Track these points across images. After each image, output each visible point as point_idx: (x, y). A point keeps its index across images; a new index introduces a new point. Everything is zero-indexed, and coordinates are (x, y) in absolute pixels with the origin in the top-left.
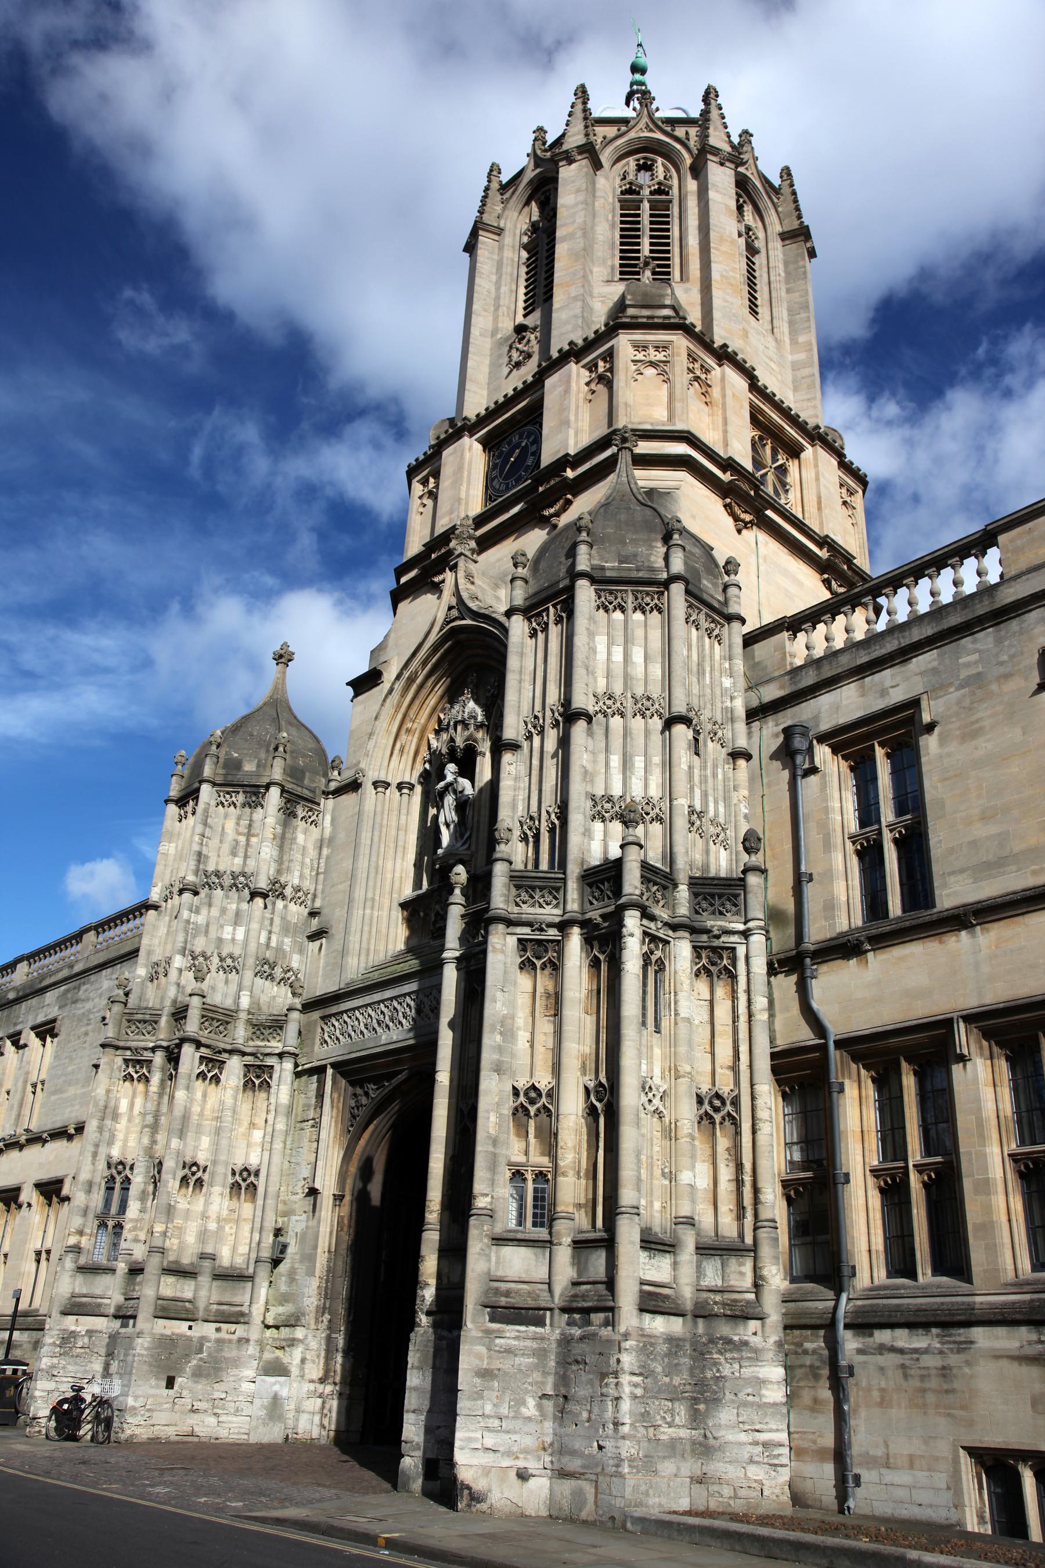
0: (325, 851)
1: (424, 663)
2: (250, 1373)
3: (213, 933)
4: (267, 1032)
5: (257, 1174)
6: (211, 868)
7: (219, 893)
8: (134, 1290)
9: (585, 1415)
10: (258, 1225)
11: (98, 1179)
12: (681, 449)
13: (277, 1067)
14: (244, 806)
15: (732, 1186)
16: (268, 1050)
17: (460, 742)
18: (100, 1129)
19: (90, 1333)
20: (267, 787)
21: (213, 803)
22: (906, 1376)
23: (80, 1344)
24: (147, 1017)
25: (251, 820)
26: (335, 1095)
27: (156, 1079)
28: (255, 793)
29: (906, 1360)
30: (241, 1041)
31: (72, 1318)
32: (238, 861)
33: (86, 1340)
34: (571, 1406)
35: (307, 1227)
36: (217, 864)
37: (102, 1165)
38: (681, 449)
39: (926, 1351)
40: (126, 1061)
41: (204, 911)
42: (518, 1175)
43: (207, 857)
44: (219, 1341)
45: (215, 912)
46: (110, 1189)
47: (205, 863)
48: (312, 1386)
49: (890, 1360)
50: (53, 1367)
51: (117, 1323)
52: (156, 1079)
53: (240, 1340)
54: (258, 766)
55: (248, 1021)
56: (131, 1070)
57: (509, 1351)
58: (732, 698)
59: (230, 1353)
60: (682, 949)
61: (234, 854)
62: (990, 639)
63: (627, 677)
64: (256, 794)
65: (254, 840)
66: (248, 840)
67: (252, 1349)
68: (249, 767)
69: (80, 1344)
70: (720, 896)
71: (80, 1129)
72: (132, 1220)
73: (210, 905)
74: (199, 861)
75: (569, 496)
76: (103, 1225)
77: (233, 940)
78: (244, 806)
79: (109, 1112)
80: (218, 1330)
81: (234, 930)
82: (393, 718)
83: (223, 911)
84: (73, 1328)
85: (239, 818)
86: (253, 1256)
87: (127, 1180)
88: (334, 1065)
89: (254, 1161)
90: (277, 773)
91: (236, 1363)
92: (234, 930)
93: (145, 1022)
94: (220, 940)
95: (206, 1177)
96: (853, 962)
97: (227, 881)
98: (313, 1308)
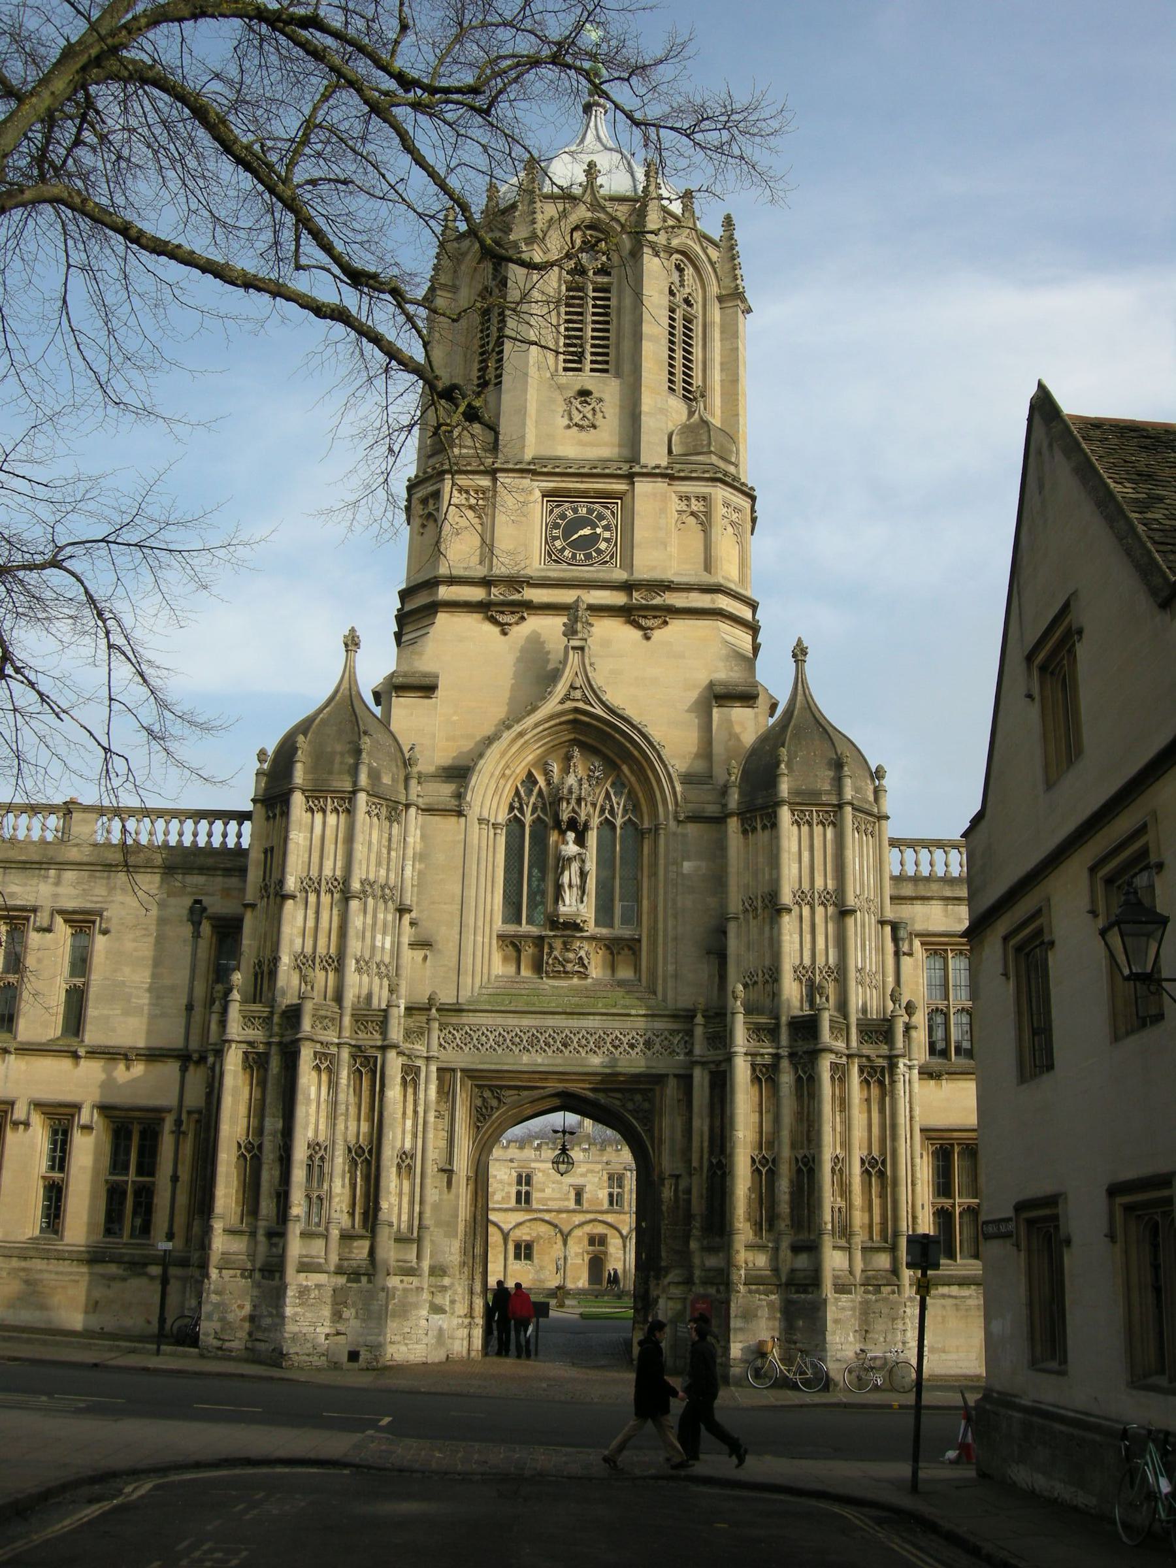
0: (417, 866)
1: (536, 725)
2: (424, 1312)
8: (351, 1252)
9: (882, 1339)
10: (417, 1199)
13: (423, 1069)
16: (418, 1054)
17: (583, 818)
19: (318, 1286)
20: (407, 806)
22: (957, 1310)
23: (312, 1296)
24: (329, 1014)
26: (464, 1095)
29: (957, 1302)
31: (303, 1275)
33: (317, 1292)
34: (869, 1336)
35: (440, 1200)
39: (970, 1297)
44: (405, 1290)
48: (460, 1321)
49: (950, 1301)
50: (296, 1314)
51: (341, 1280)
53: (417, 1288)
57: (843, 1309)
59: (412, 1299)
67: (425, 1295)
69: (312, 1296)
72: (339, 1195)
77: (383, 948)
80: (402, 1281)
82: (498, 763)
84: (305, 1283)
86: (416, 1223)
88: (462, 1070)
89: (408, 1146)
91: (416, 1306)
96: (932, 1082)
98: (457, 1263)
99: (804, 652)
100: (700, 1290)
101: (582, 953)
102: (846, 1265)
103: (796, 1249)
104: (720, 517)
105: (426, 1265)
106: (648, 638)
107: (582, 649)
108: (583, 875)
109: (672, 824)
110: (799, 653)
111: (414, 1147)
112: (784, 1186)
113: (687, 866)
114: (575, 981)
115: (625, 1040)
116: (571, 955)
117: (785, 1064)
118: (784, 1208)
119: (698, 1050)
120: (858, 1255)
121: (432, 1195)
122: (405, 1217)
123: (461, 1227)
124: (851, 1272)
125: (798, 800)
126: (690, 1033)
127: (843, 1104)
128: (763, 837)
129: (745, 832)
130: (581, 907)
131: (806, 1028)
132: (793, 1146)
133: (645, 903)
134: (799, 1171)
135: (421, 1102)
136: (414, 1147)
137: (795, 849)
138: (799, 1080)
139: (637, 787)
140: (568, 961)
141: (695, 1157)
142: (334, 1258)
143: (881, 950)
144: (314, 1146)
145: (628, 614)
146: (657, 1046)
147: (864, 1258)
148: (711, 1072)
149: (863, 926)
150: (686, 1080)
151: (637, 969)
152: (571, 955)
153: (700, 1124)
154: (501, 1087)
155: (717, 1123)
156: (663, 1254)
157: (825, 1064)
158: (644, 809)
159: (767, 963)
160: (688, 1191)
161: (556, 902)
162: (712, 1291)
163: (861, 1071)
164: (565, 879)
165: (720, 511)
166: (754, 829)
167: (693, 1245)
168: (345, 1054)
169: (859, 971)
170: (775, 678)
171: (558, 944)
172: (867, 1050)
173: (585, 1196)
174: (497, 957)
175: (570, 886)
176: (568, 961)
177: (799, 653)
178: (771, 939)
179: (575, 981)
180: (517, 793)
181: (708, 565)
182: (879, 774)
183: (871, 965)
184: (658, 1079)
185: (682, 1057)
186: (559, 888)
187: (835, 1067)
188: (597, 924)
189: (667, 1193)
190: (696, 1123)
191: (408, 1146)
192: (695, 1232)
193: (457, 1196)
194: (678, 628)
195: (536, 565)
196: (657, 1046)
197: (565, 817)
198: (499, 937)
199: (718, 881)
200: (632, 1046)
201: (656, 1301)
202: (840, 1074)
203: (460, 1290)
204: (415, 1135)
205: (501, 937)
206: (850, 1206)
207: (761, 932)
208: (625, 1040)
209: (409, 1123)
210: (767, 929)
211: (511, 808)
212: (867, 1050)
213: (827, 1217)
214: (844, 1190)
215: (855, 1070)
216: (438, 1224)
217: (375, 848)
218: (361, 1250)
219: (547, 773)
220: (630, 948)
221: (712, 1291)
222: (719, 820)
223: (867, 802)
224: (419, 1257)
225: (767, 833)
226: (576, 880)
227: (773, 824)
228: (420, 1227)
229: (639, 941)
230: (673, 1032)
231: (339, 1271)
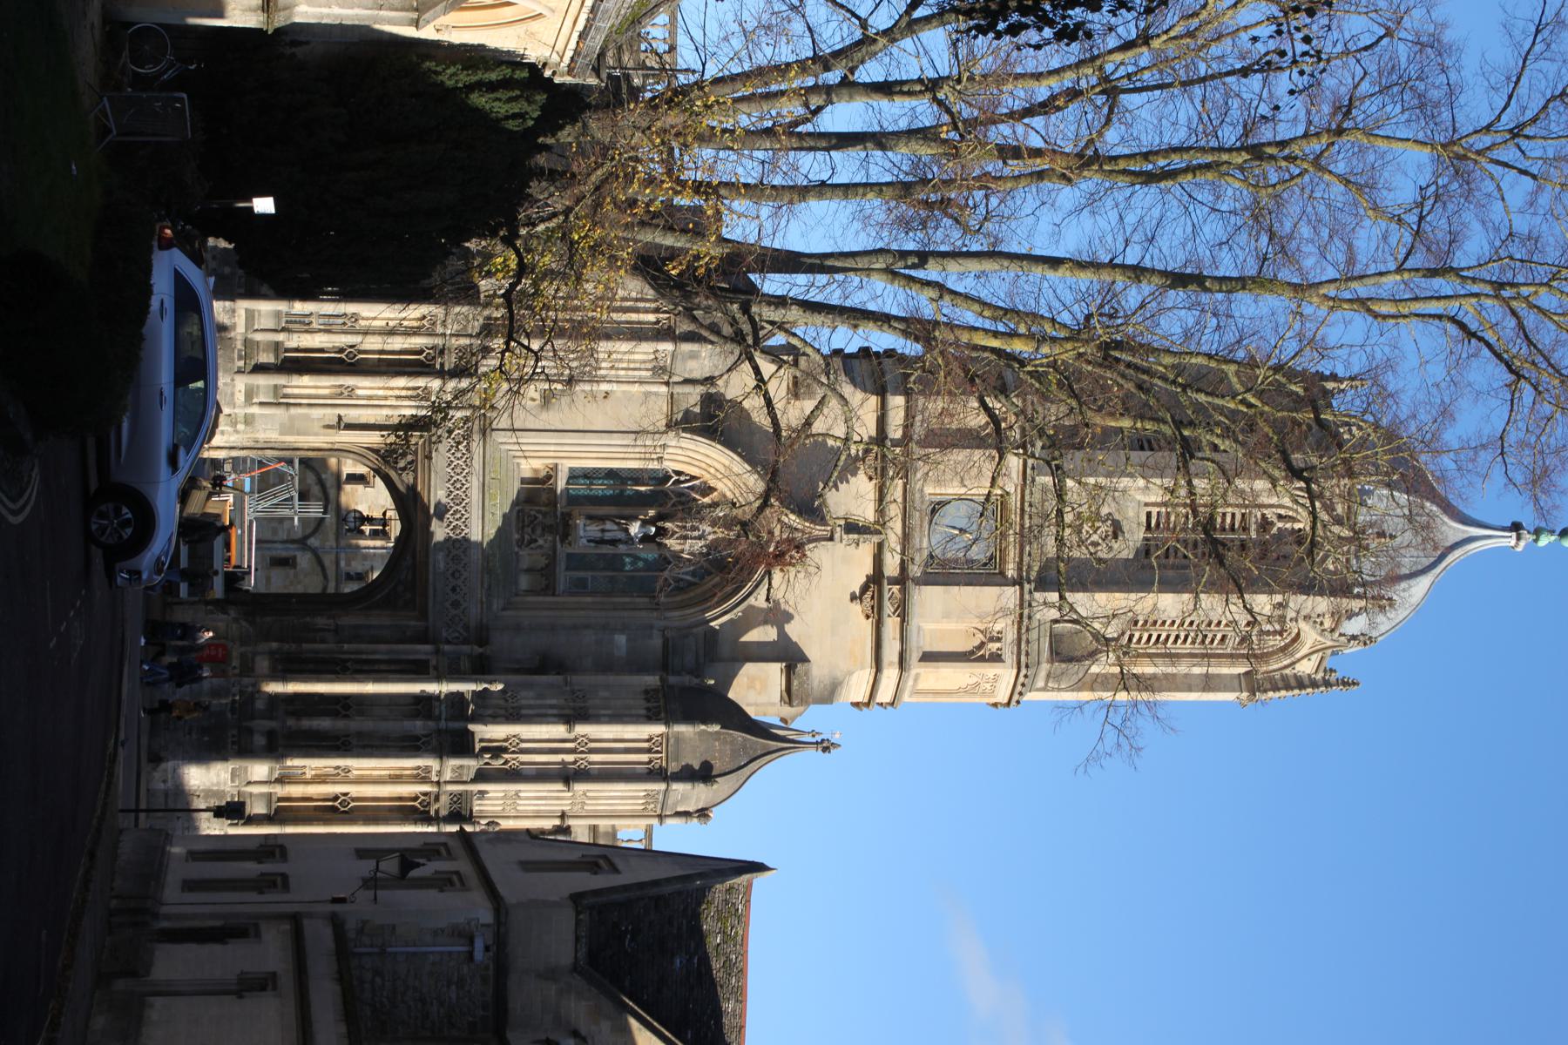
99: (825, 749)
100: (235, 654)
101: (541, 542)
102: (255, 778)
103: (270, 735)
104: (982, 671)
105: (255, 410)
106: (853, 598)
107: (831, 539)
108: (614, 542)
109: (662, 623)
110: (826, 746)
111: (359, 398)
112: (324, 724)
113: (621, 640)
114: (516, 536)
115: (459, 582)
116: (539, 531)
117: (431, 724)
118: (306, 723)
119: (447, 648)
120: (264, 789)
121: (316, 413)
122: (296, 391)
123: (290, 439)
124: (249, 783)
125: (672, 741)
126: (466, 642)
127: (396, 779)
128: (640, 705)
129: (646, 692)
130: (584, 541)
131: (461, 745)
132: (360, 734)
133: (589, 599)
134: (337, 738)
135: (399, 403)
136: (359, 398)
137: (626, 736)
138: (417, 738)
139: (699, 591)
140: (533, 531)
141: (354, 646)
142: (259, 337)
143: (538, 816)
144: (355, 317)
145: (876, 579)
146: (454, 612)
147: (262, 795)
148: (427, 662)
149: (558, 798)
150: (423, 637)
151: (531, 592)
152: (539, 531)
153: (382, 651)
154: (415, 471)
155: (383, 667)
156: (268, 619)
157: (432, 763)
158: (678, 598)
159: (524, 712)
160: (323, 641)
161: (590, 517)
162: (236, 663)
163: (425, 794)
164: (609, 525)
165: (990, 670)
166: (648, 700)
167: (275, 645)
168: (439, 341)
169: (517, 793)
170: (809, 719)
171: (549, 521)
172: (444, 799)
173: (360, 488)
174: (538, 464)
175: (603, 531)
176: (533, 531)
177: (826, 746)
178: (546, 715)
179: (516, 536)
180: (693, 478)
181: (929, 657)
182: (703, 813)
183: (525, 806)
184: (424, 615)
185: (444, 634)
186: (602, 519)
187: (428, 769)
188: (570, 556)
189: (321, 621)
190: (383, 647)
191: (359, 392)
192: (286, 646)
193: (316, 434)
194: (867, 626)
195: (929, 490)
196: (454, 612)
197: (668, 525)
198: (555, 468)
199: (607, 665)
200: (454, 590)
201: (226, 613)
202: (421, 777)
203: (232, 438)
204: (370, 398)
205: (555, 468)
206: (307, 783)
207: (552, 707)
208: (459, 582)
209: (381, 393)
210: (555, 712)
211: (679, 473)
212: (444, 799)
213: (297, 762)
214: (320, 779)
215: (426, 788)
216: (292, 418)
217: (626, 357)
218: (266, 358)
219: (715, 505)
220: (547, 587)
221: (236, 663)
222: (665, 666)
223: (676, 804)
224: (261, 404)
225: (643, 712)
226: (608, 536)
227: (651, 718)
228: (288, 405)
229: (554, 595)
230: (466, 627)
231: (246, 341)
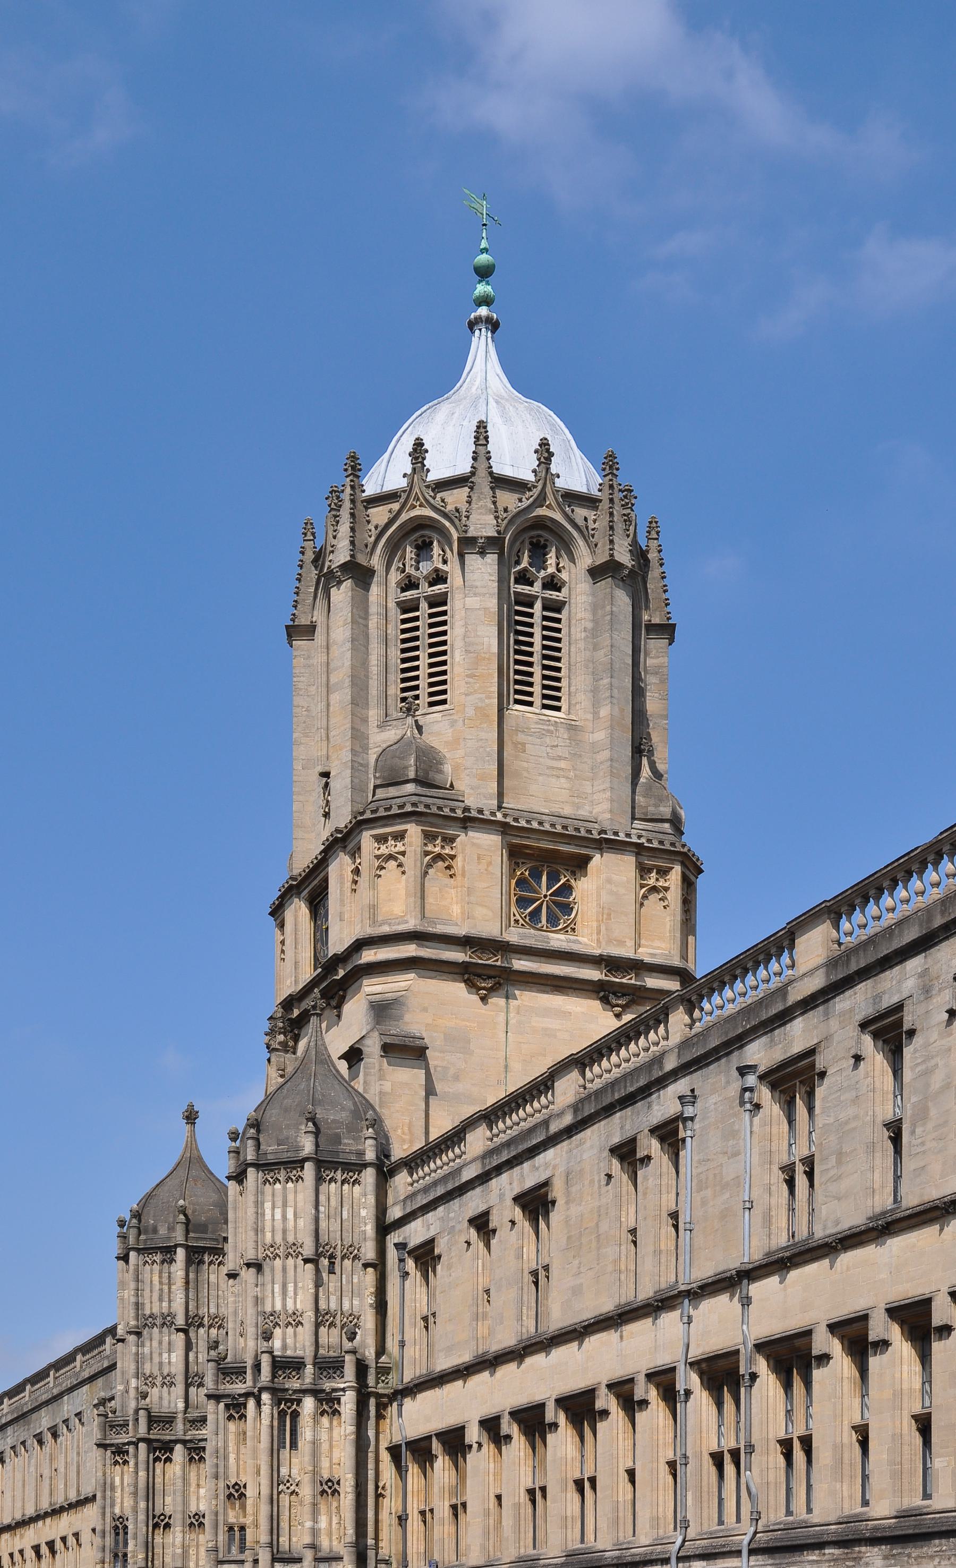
3: (156, 1359)
4: (199, 1424)
5: (204, 1516)
6: (148, 1312)
7: (156, 1330)
11: (108, 1528)
12: (410, 950)
14: (163, 1262)
15: (337, 1526)
18: (104, 1498)
21: (141, 1263)
25: (169, 1273)
27: (132, 1463)
28: (168, 1252)
30: (182, 1433)
32: (165, 1304)
36: (151, 1308)
37: (108, 1519)
38: (410, 950)
40: (113, 1453)
41: (147, 1344)
42: (231, 1529)
43: (143, 1304)
45: (155, 1344)
46: (117, 1534)
47: (143, 1309)
52: (132, 1463)
54: (169, 1229)
55: (185, 1419)
56: (117, 1458)
58: (366, 1224)
60: (309, 1404)
61: (161, 1300)
62: (458, 1205)
63: (284, 1231)
64: (170, 1252)
65: (173, 1287)
66: (170, 1288)
68: (163, 1231)
70: (334, 1368)
71: (94, 1496)
73: (151, 1340)
74: (138, 1309)
75: (341, 993)
76: (116, 1556)
78: (163, 1262)
79: (107, 1486)
81: (169, 1355)
83: (160, 1343)
85: (161, 1272)
87: (126, 1527)
90: (179, 1236)
92: (169, 1355)
93: (121, 1425)
94: (161, 1364)
95: (171, 1522)
97: (158, 1322)
